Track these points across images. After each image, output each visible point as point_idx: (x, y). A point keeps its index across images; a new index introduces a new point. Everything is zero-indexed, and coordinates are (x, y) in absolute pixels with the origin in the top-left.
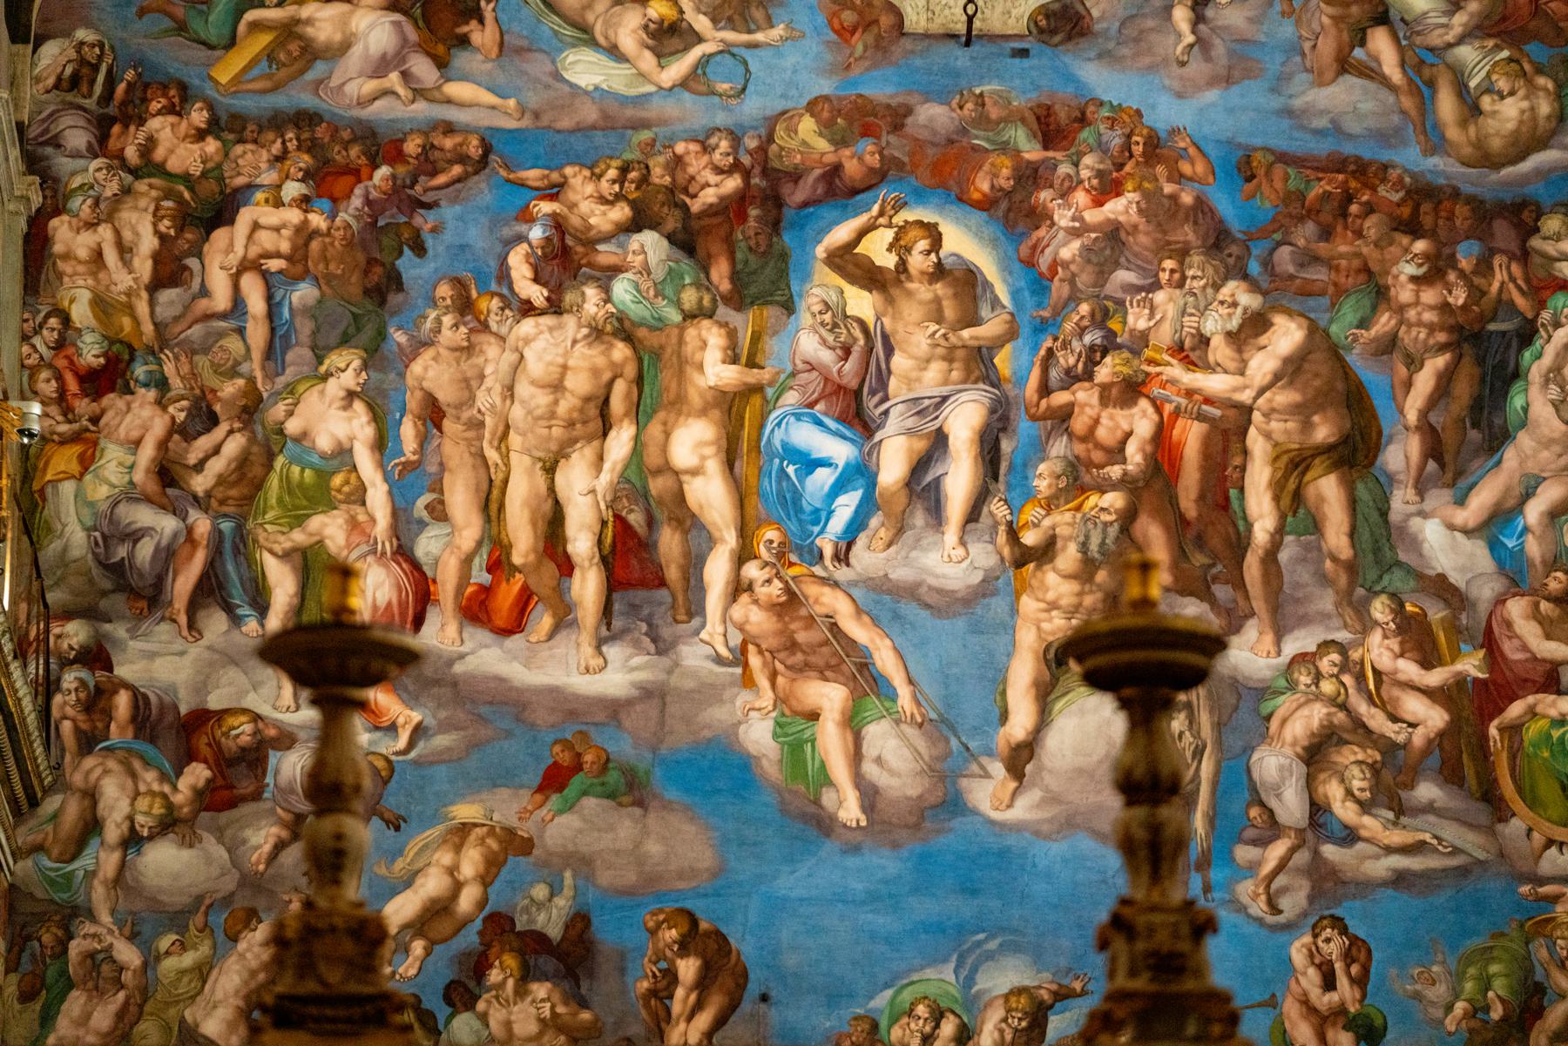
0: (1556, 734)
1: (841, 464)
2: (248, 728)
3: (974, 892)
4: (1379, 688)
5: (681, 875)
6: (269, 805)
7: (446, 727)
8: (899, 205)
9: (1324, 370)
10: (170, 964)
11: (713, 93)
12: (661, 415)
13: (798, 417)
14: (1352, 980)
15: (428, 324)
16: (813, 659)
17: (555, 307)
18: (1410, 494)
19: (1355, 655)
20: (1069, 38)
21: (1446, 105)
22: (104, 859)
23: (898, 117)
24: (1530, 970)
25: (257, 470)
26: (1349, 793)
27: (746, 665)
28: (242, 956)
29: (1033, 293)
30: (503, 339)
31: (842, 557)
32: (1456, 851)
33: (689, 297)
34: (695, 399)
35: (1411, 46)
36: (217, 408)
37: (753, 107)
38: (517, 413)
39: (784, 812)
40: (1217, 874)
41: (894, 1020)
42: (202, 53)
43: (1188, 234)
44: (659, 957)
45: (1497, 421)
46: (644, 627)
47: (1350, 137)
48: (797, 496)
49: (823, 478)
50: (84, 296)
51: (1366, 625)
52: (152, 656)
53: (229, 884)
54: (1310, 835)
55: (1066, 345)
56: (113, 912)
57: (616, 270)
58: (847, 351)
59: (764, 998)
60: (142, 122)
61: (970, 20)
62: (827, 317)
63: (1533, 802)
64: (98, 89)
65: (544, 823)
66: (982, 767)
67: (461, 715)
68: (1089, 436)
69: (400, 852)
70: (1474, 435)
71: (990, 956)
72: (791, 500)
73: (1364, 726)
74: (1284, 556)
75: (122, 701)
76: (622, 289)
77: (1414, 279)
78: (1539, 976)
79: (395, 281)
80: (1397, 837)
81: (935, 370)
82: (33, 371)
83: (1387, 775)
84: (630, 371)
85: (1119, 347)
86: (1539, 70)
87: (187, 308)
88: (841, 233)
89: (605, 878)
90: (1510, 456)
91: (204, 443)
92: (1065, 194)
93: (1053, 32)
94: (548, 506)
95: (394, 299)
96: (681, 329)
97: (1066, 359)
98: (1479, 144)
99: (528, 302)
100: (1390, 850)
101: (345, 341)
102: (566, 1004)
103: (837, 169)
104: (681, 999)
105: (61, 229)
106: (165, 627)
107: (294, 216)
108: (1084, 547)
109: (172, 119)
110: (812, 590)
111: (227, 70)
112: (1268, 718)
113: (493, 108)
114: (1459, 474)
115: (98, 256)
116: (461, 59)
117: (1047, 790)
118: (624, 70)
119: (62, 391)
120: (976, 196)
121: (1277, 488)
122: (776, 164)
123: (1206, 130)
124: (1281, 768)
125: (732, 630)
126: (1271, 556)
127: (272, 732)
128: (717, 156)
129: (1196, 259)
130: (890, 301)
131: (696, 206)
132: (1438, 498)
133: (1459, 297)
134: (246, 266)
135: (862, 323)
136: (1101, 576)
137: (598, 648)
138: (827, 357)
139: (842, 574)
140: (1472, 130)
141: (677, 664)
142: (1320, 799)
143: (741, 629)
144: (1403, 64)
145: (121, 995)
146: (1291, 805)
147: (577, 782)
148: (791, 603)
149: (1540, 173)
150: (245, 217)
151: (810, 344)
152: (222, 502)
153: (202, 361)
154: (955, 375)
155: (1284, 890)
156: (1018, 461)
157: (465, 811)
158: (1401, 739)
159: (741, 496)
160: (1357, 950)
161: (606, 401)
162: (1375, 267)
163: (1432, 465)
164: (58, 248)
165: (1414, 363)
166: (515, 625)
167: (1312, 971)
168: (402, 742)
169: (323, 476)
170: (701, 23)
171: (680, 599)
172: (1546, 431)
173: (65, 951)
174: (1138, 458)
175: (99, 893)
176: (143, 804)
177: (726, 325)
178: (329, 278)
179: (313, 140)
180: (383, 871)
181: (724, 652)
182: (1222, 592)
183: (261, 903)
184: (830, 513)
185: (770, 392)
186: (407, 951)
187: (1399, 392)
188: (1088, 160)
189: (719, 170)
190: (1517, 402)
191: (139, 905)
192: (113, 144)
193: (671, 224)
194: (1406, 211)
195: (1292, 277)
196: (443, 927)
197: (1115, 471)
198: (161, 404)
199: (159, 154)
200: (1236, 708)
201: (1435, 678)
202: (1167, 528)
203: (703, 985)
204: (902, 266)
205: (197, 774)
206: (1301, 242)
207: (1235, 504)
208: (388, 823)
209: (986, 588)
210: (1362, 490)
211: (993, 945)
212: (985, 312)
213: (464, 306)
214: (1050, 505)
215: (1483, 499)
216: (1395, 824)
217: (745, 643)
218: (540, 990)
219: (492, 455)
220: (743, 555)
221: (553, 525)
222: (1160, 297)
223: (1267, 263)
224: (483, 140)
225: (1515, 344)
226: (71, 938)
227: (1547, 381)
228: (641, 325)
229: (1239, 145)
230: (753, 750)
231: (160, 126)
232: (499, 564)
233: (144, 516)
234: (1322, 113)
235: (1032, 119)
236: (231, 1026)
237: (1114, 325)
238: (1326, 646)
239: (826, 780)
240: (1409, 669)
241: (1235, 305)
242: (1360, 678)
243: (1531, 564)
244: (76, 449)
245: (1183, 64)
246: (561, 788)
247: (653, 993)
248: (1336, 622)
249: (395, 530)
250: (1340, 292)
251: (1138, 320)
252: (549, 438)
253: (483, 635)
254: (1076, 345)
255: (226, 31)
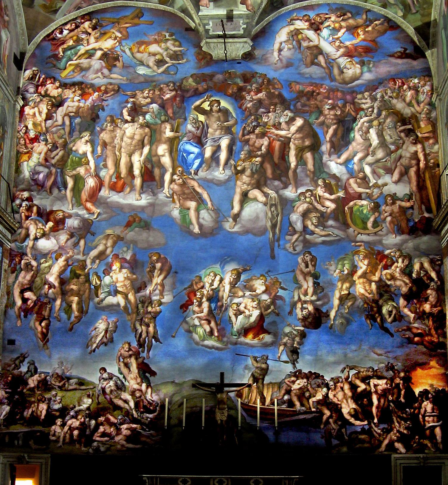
0: (361, 209)
1: (196, 153)
2: (62, 214)
3: (224, 248)
4: (320, 200)
5: (157, 245)
6: (65, 231)
7: (105, 213)
8: (211, 96)
9: (308, 129)
10: (43, 265)
11: (170, 74)
12: (156, 143)
13: (187, 143)
14: (312, 266)
15: (105, 126)
16: (189, 196)
17: (133, 121)
18: (327, 156)
19: (314, 192)
20: (250, 59)
21: (336, 71)
22: (29, 243)
23: (211, 76)
24: (354, 263)
25: (65, 158)
26: (312, 224)
27: (173, 198)
28: (59, 264)
29: (241, 114)
30: (121, 128)
31: (196, 173)
32: (337, 236)
33: (163, 118)
34: (163, 139)
35: (328, 59)
36: (58, 145)
37: (179, 76)
38: (123, 144)
39: (181, 230)
40: (281, 242)
41: (205, 277)
42: (59, 71)
43: (276, 100)
44: (151, 263)
45: (348, 140)
46: (150, 190)
47: (314, 79)
48: (186, 160)
49: (192, 156)
50: (31, 123)
51: (317, 185)
52: (42, 199)
53: (56, 248)
54: (303, 233)
55: (248, 125)
56: (31, 254)
57: (146, 113)
58: (198, 128)
59: (176, 272)
60: (45, 86)
61: (226, 54)
62: (194, 121)
63: (355, 224)
64: (37, 79)
65: (126, 234)
66: (227, 220)
67: (109, 211)
68: (253, 145)
69: (94, 241)
70: (342, 142)
71: (228, 262)
72: (184, 160)
73: (316, 208)
74: (298, 171)
75: (35, 209)
76: (148, 117)
77: (328, 109)
78: (356, 263)
79: (98, 117)
80: (323, 233)
81: (218, 132)
82: (20, 139)
83: (321, 219)
84: (149, 134)
85: (261, 126)
86: (357, 63)
87: (52, 124)
88: (198, 103)
89: (140, 245)
90: (350, 147)
91: (55, 153)
92: (249, 93)
93: (246, 58)
94: (129, 164)
95: (98, 120)
96: (161, 124)
97: (248, 129)
98: (343, 79)
99: (127, 120)
100: (322, 236)
101: (86, 130)
102: (130, 273)
103: (197, 89)
104: (156, 273)
105: (27, 110)
106: (45, 192)
107: (76, 104)
108: (252, 170)
109: (52, 85)
110: (189, 181)
111: (64, 74)
112: (294, 207)
113: (121, 79)
114: (339, 150)
115: (35, 114)
116: (114, 70)
117: (242, 224)
118: (150, 70)
119: (25, 142)
120: (228, 94)
121: (297, 156)
122: (183, 88)
123: (281, 78)
124: (297, 218)
125: (170, 190)
126: (295, 171)
127: (67, 215)
128: (170, 87)
129: (279, 106)
130: (208, 117)
131: (165, 98)
132: (334, 157)
133: (339, 113)
134: (66, 115)
135: (201, 122)
136: (256, 176)
137: (140, 196)
138: (193, 129)
139: (196, 177)
140: (342, 77)
141: (157, 198)
142: (305, 225)
143: (172, 190)
144: (326, 63)
145: (33, 272)
146: (299, 226)
147: (134, 225)
148: (184, 184)
149: (357, 86)
150: (66, 105)
151: (190, 127)
152: (58, 165)
153: (55, 136)
154: (223, 133)
155: (297, 246)
156: (237, 151)
157: (109, 232)
158: (325, 211)
159: (173, 160)
160: (314, 259)
161: (144, 141)
162: (319, 106)
163: (332, 150)
164: (26, 113)
165: (328, 127)
166: (121, 190)
167: (303, 264)
168: (95, 217)
169: (80, 159)
170: (168, 59)
171: (159, 183)
172: (359, 142)
173: (21, 263)
174: (265, 150)
175: (28, 250)
176: (38, 231)
177: (170, 124)
178: (83, 117)
179: (82, 88)
180: (90, 245)
181: (168, 195)
182: (283, 179)
183: (63, 252)
184: (194, 164)
185: (180, 138)
186: (95, 263)
187: (325, 134)
188: (254, 85)
189: (171, 90)
190: (352, 135)
191: (37, 253)
192: (39, 91)
193: (159, 102)
194: (326, 94)
195: (300, 109)
196: (104, 257)
197: (259, 153)
198: (46, 145)
199: (49, 92)
200: (286, 205)
201: (333, 197)
202: (271, 165)
203: (161, 270)
204: (211, 109)
205: (50, 224)
206: (303, 102)
207: (287, 159)
208: (92, 234)
209: (228, 180)
210: (316, 156)
211: (228, 259)
212: (230, 119)
213: (113, 121)
214: (244, 161)
215: (344, 157)
216: (323, 230)
217: (173, 193)
218: (124, 271)
219: (117, 153)
220: (173, 174)
221: (130, 168)
222: (270, 114)
223: (295, 106)
224: (118, 86)
225: (352, 122)
226: (22, 259)
227: (359, 131)
228: (152, 124)
229: (289, 81)
230: (174, 217)
231: (49, 86)
232: (118, 177)
233: (41, 169)
234: (307, 74)
235: (241, 77)
236: (56, 279)
237: (259, 121)
238: (308, 191)
239: (191, 223)
240: (327, 195)
241: (287, 116)
242: (315, 198)
243: (355, 171)
244: (28, 155)
245: (276, 64)
246: (130, 226)
247: (150, 271)
248: (310, 185)
249: (95, 170)
250: (311, 112)
251: (265, 119)
252: (130, 149)
253: (114, 193)
254: (251, 126)
255: (64, 66)
